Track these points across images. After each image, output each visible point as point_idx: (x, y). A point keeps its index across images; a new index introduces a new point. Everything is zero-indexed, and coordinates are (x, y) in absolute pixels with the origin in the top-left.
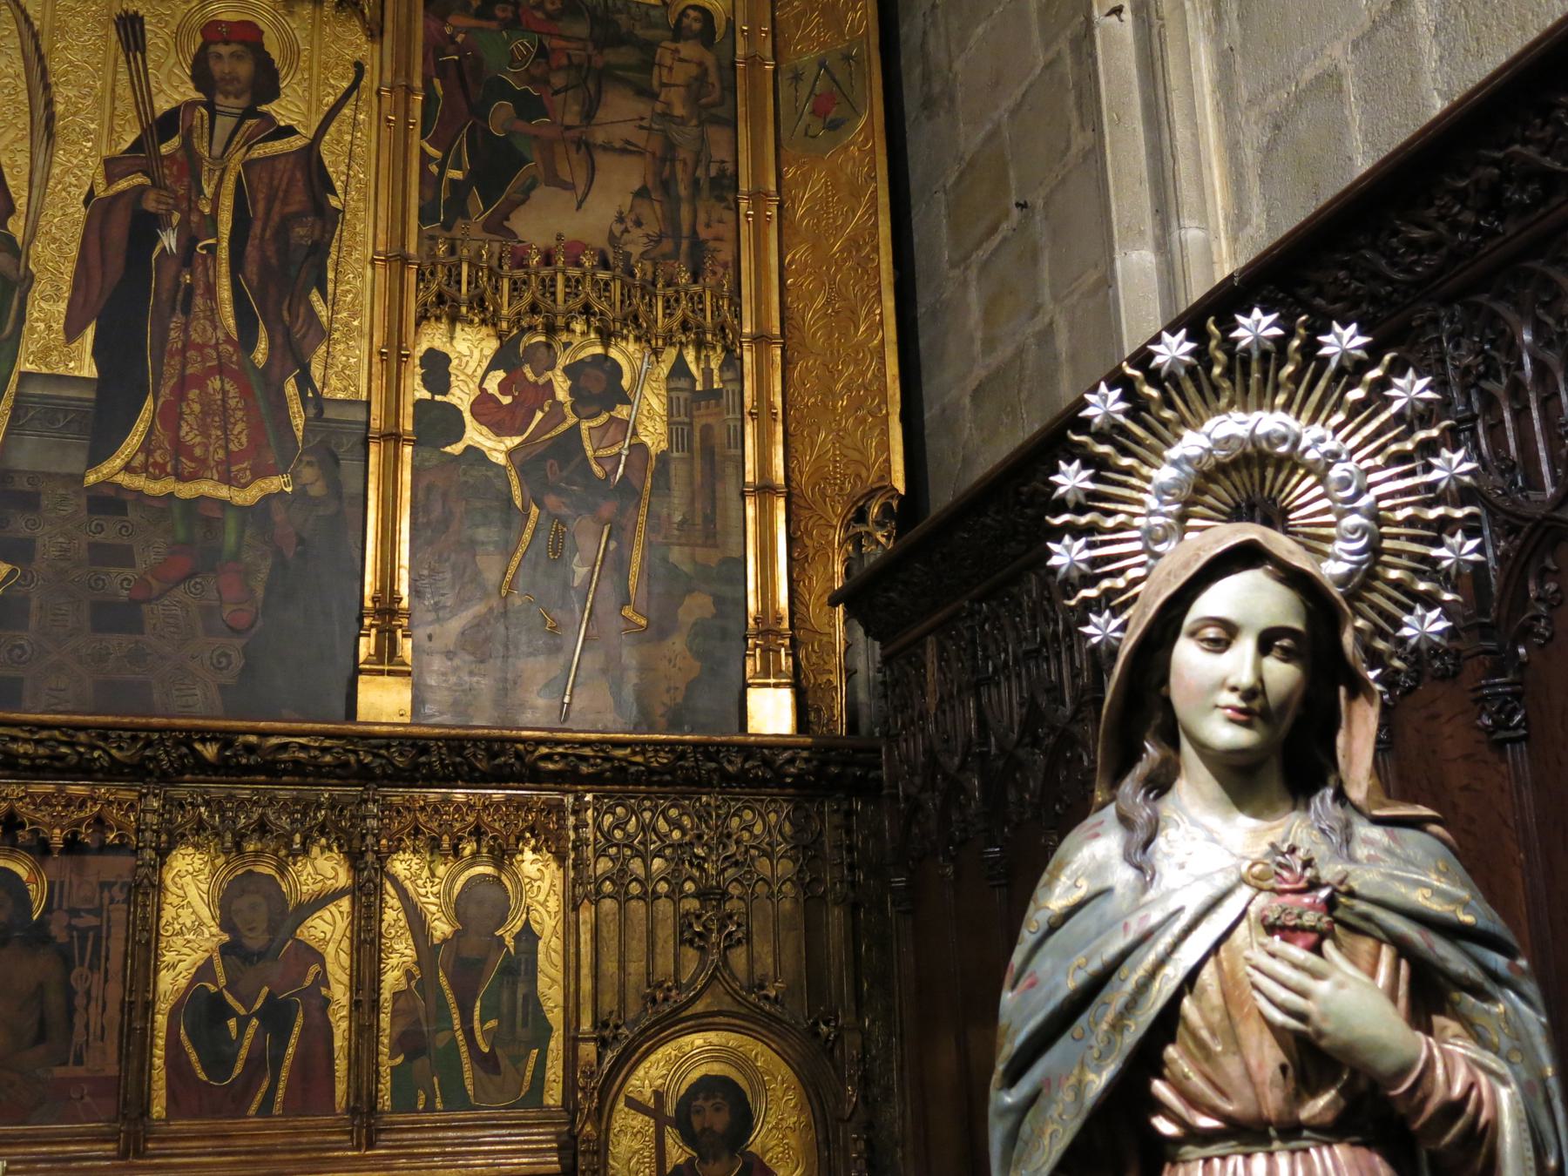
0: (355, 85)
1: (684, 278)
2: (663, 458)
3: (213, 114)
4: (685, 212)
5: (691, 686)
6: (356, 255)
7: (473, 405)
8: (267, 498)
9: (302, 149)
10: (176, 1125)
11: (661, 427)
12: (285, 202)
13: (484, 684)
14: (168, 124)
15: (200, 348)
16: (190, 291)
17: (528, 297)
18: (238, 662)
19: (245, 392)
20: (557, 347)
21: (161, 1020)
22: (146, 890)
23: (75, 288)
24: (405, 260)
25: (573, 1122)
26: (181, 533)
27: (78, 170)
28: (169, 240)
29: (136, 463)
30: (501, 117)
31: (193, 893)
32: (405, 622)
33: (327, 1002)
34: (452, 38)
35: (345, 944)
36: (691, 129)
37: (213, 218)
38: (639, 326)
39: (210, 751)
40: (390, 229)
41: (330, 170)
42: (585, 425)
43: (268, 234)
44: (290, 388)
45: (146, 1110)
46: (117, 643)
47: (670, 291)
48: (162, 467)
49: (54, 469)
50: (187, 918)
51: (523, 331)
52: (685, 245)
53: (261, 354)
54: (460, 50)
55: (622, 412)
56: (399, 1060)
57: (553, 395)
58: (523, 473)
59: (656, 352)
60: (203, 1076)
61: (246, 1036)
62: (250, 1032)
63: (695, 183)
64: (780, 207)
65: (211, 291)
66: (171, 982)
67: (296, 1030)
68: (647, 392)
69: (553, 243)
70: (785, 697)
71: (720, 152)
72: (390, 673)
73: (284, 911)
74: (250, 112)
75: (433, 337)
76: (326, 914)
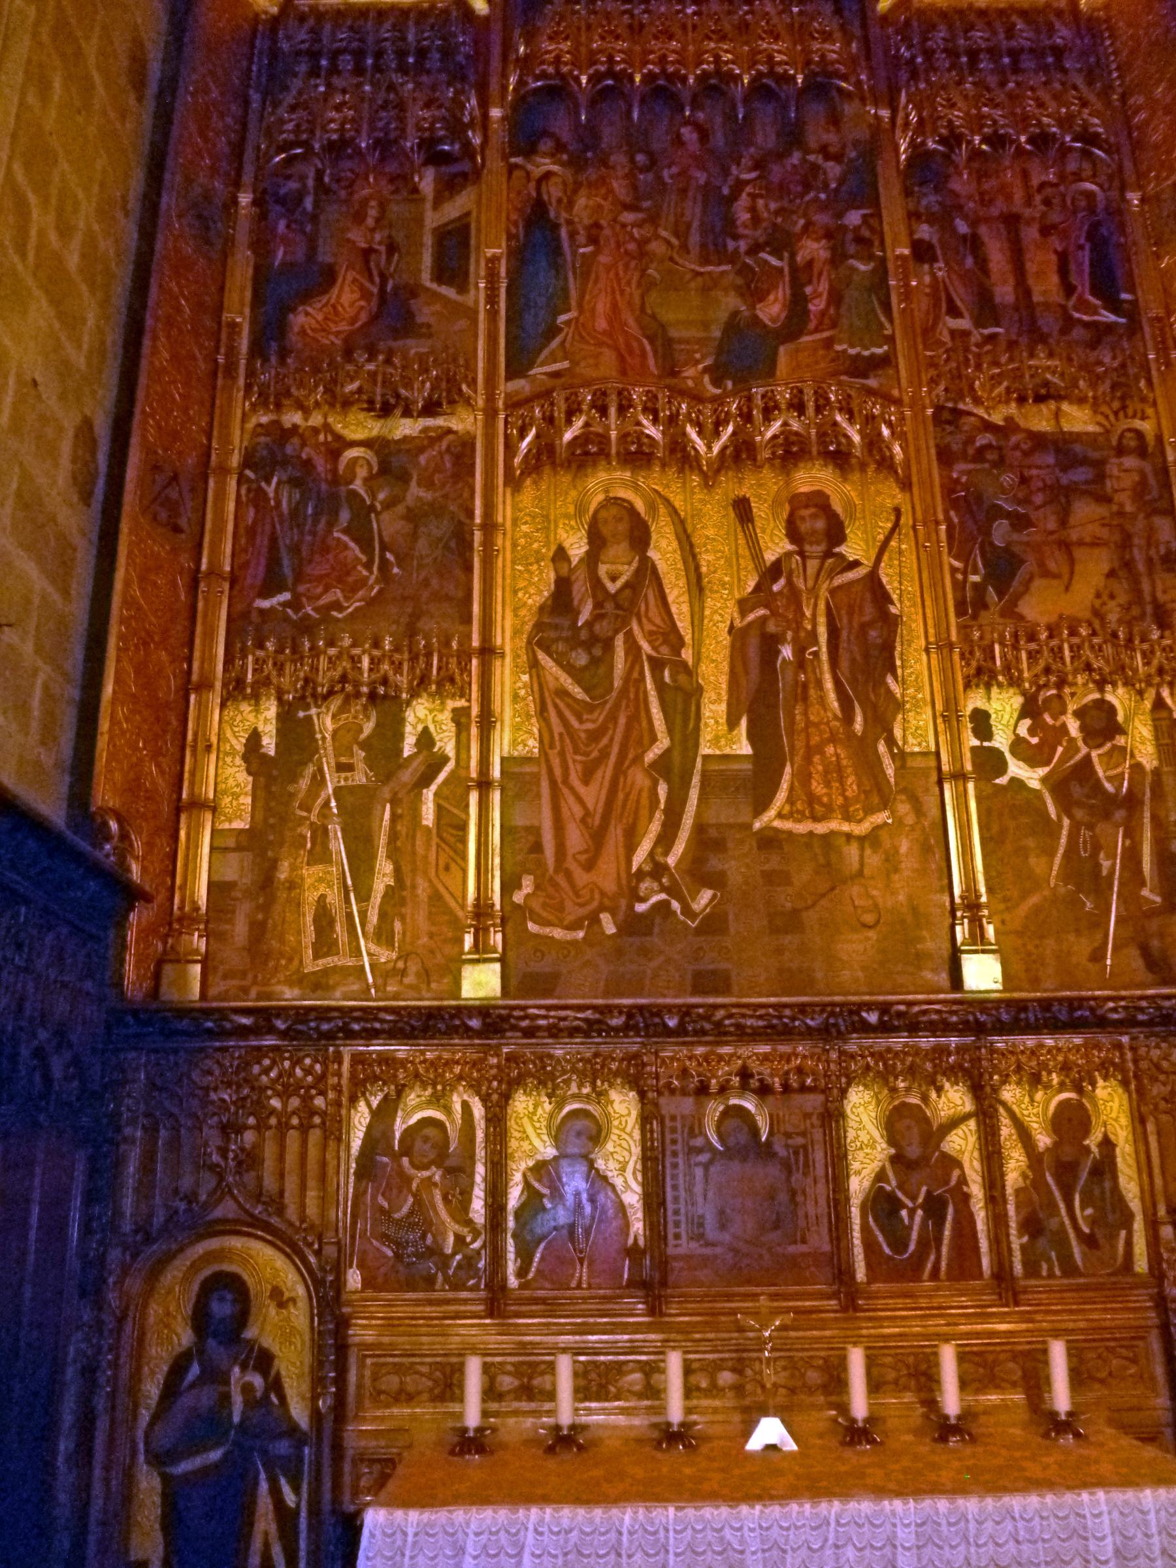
0: (896, 525)
2: (1156, 772)
4: (1146, 586)
8: (877, 828)
10: (875, 1287)
11: (1150, 749)
12: (861, 614)
14: (776, 570)
15: (816, 725)
16: (805, 686)
17: (1042, 664)
20: (1068, 699)
21: (855, 1212)
24: (951, 646)
25: (1160, 1285)
27: (722, 612)
28: (787, 652)
30: (1001, 533)
33: (967, 1197)
35: (976, 1154)
40: (937, 626)
42: (1094, 754)
44: (882, 748)
45: (853, 1277)
46: (789, 940)
47: (1145, 646)
48: (802, 813)
50: (864, 1137)
51: (1039, 688)
52: (1149, 609)
54: (966, 487)
55: (1120, 740)
56: (1025, 1239)
59: (1141, 693)
60: (887, 1250)
61: (915, 1221)
63: (1150, 561)
65: (819, 684)
66: (858, 1185)
67: (949, 1218)
68: (1137, 723)
69: (1053, 618)
74: (828, 554)
75: (975, 700)
76: (959, 1131)
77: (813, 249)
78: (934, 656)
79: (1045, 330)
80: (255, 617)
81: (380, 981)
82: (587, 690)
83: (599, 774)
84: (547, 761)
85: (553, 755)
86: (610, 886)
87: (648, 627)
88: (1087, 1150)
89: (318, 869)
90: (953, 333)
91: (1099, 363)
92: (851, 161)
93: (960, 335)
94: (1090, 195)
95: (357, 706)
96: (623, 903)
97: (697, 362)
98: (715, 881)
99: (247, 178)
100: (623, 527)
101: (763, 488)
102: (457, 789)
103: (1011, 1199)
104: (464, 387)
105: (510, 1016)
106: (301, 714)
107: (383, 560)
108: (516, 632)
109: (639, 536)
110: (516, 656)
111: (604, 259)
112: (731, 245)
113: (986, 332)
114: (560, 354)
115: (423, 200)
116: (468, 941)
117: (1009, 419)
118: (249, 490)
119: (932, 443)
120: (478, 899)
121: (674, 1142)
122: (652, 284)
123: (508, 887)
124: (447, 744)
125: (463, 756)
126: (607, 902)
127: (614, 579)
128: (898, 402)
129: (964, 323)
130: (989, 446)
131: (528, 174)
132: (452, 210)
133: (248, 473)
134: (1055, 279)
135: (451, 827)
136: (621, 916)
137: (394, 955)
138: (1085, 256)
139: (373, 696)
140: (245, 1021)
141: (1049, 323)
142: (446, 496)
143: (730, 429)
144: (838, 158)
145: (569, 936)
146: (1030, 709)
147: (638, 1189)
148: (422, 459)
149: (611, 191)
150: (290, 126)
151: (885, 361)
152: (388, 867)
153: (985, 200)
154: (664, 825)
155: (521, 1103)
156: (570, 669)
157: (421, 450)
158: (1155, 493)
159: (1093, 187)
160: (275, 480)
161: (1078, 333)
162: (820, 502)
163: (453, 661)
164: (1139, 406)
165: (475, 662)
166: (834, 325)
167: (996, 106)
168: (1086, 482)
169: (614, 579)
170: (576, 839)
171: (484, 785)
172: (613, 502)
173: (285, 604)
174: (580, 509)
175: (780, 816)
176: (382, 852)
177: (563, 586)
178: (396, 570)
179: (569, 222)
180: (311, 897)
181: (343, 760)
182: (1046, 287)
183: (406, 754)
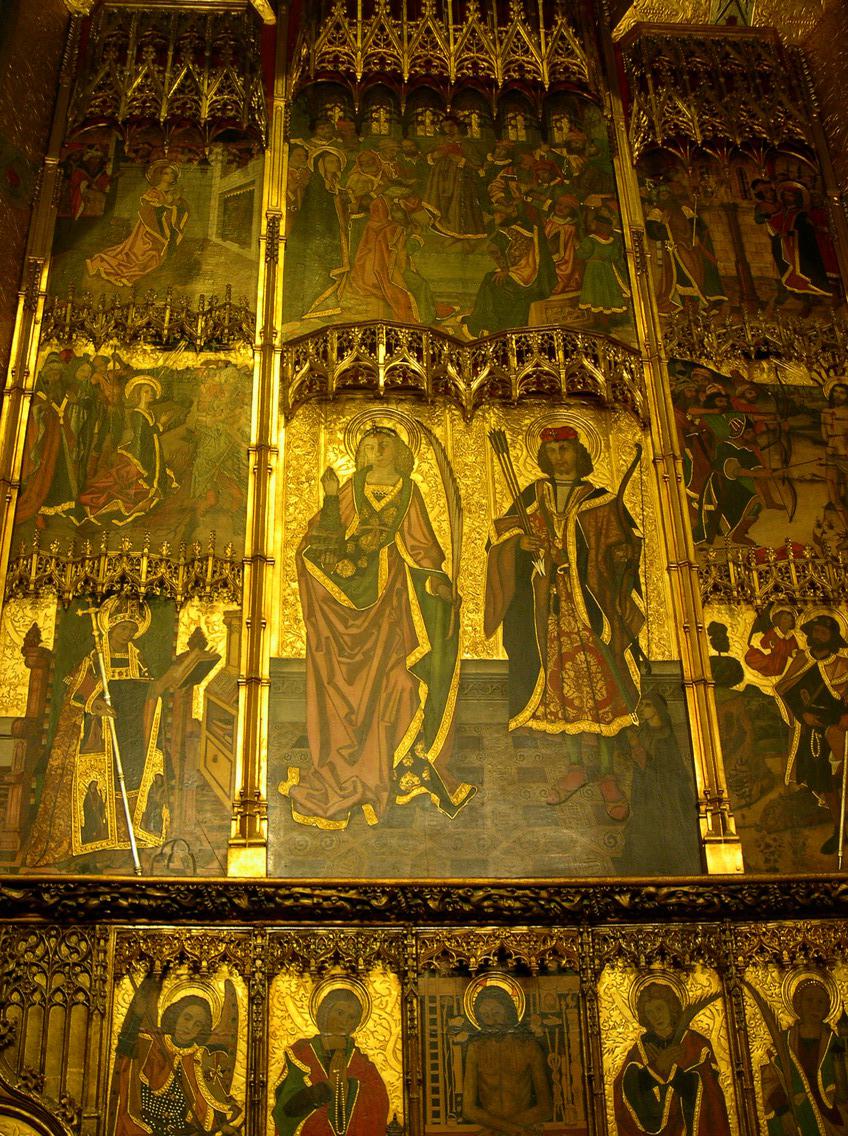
0: (638, 458)
3: (555, 485)
7: (746, 657)
8: (623, 731)
9: (612, 501)
12: (607, 537)
14: (528, 495)
15: (569, 635)
16: (557, 598)
17: (771, 584)
19: (601, 662)
21: (609, 1089)
22: (588, 998)
23: (487, 603)
24: (690, 566)
27: (479, 530)
28: (540, 567)
29: (538, 713)
30: (730, 469)
31: (619, 1002)
33: (716, 1074)
34: (692, 421)
35: (723, 1032)
37: (565, 550)
39: (624, 900)
41: (631, 513)
42: (821, 665)
43: (600, 558)
48: (555, 714)
49: (489, 721)
50: (616, 1017)
53: (606, 635)
54: (699, 428)
56: (772, 1115)
57: (797, 646)
58: (786, 698)
60: (641, 1128)
62: (669, 1097)
65: (570, 597)
69: (781, 544)
72: (726, 842)
73: (679, 1012)
75: (715, 614)
77: (560, 224)
79: (763, 298)
82: (351, 597)
83: (364, 673)
84: (314, 660)
85: (320, 657)
86: (372, 781)
87: (411, 542)
88: (828, 1028)
89: (90, 758)
90: (682, 298)
92: (591, 155)
96: (385, 795)
97: (459, 313)
102: (227, 687)
103: (757, 1076)
105: (276, 894)
106: (80, 613)
107: (163, 472)
108: (286, 544)
110: (285, 565)
111: (375, 224)
112: (487, 218)
116: (235, 827)
117: (735, 373)
120: (245, 788)
121: (433, 1022)
122: (416, 247)
123: (277, 776)
124: (218, 640)
125: (234, 654)
126: (370, 795)
127: (379, 498)
128: (637, 353)
129: (694, 291)
130: (718, 394)
133: (40, 394)
134: (769, 258)
135: (220, 718)
140: (15, 894)
141: (763, 294)
143: (486, 372)
144: (580, 152)
146: (762, 624)
147: (399, 1068)
154: (424, 723)
155: (286, 985)
156: (336, 578)
159: (799, 186)
160: (65, 401)
161: (790, 303)
162: (567, 435)
165: (247, 569)
166: (579, 287)
167: (715, 115)
168: (803, 428)
169: (379, 498)
170: (340, 735)
171: (253, 681)
173: (68, 512)
175: (534, 716)
176: (153, 742)
177: (331, 501)
178: (175, 485)
181: (118, 656)
182: (762, 264)
183: (179, 652)
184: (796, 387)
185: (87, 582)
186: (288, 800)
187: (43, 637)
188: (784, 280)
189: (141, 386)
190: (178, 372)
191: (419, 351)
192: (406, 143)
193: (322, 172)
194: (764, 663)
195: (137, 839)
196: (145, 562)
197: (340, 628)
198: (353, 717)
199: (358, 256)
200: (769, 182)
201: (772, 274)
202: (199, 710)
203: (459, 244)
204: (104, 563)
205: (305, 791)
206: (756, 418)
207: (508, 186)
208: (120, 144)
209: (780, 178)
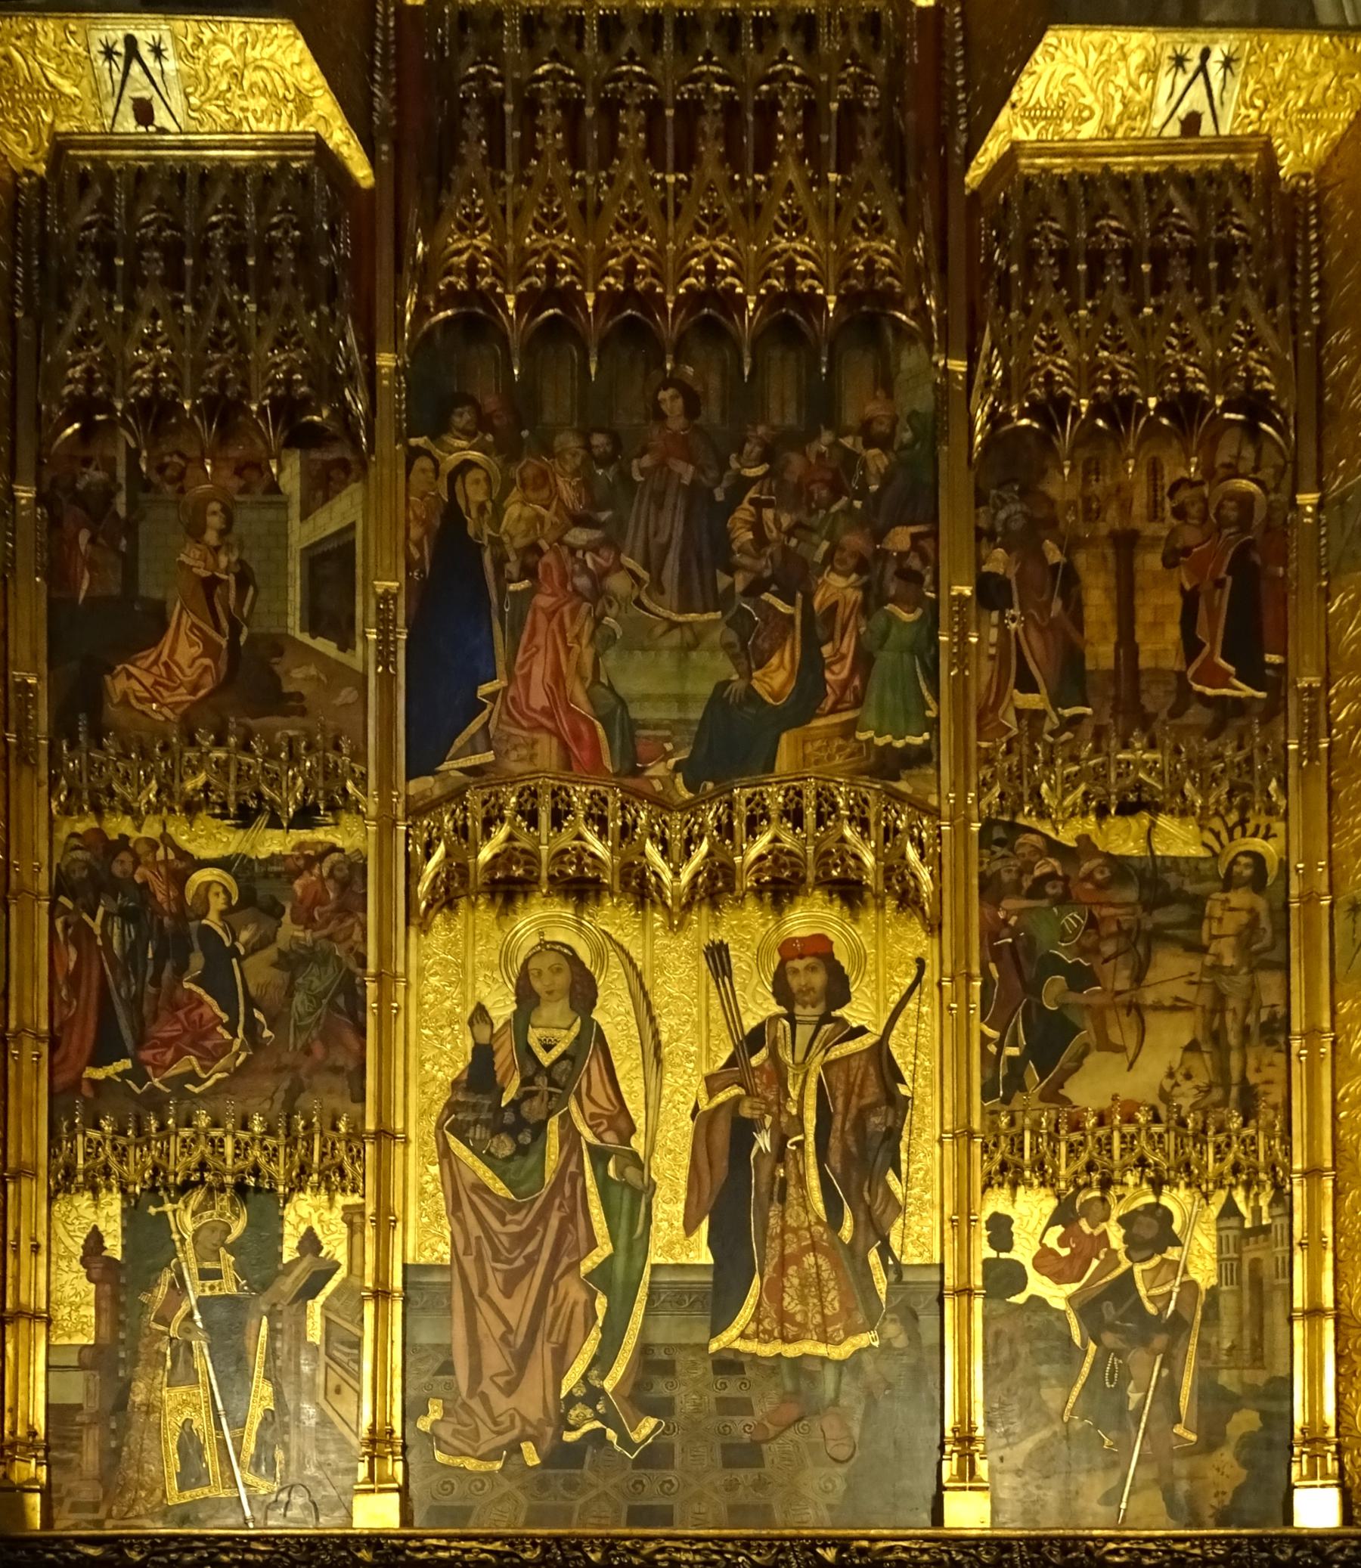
1: (1235, 1124)
2: (1213, 1293)
4: (1235, 1061)
5: (1239, 1492)
6: (925, 1136)
12: (861, 1096)
13: (1052, 1496)
14: (755, 1039)
15: (795, 1231)
16: (784, 1182)
17: (1084, 1157)
18: (841, 1486)
19: (835, 1265)
23: (690, 1189)
24: (971, 1135)
26: (789, 1385)
27: (684, 1090)
28: (764, 1141)
30: (1054, 991)
32: (981, 1447)
34: (1005, 921)
36: (1242, 978)
37: (800, 1117)
38: (1189, 1173)
40: (955, 1110)
42: (1138, 1269)
44: (874, 1258)
46: (745, 1475)
48: (770, 1333)
51: (1079, 1189)
52: (1234, 1092)
53: (846, 1232)
54: (1014, 932)
55: (1173, 1253)
57: (1107, 1244)
59: (1206, 1196)
63: (1245, 1031)
64: (1334, 1043)
65: (802, 1181)
68: (1197, 1233)
69: (1107, 1103)
70: (1333, 1495)
71: (1271, 996)
74: (826, 1018)
75: (997, 1202)
77: (837, 587)
78: (948, 1147)
79: (1150, 708)
80: (87, 1091)
81: (259, 1516)
82: (510, 1186)
83: (525, 1282)
85: (468, 1262)
86: (534, 1413)
90: (1020, 713)
91: (1218, 757)
92: (904, 447)
93: (1037, 716)
94: (1245, 501)
95: (223, 1201)
96: (550, 1431)
97: (668, 755)
98: (661, 1409)
99: (26, 461)
100: (563, 980)
101: (748, 930)
104: (349, 784)
106: (152, 1210)
107: (249, 1016)
108: (423, 1114)
109: (583, 992)
111: (543, 601)
113: (1067, 712)
114: (480, 741)
115: (285, 506)
116: (363, 1470)
117: (1084, 839)
118: (66, 926)
119: (975, 870)
120: (374, 1424)
124: (335, 1245)
125: (357, 1261)
127: (548, 1048)
128: (935, 813)
129: (1033, 701)
130: (1052, 876)
131: (436, 463)
132: (329, 520)
133: (62, 899)
134: (1173, 632)
136: (546, 1446)
137: (276, 1487)
138: (1223, 600)
139: (241, 1189)
141: (1156, 699)
142: (330, 937)
143: (705, 847)
144: (885, 443)
145: (485, 1466)
148: (298, 885)
149: (555, 493)
150: (77, 372)
151: (925, 756)
152: (267, 1390)
153: (1091, 512)
156: (489, 1159)
157: (298, 873)
158: (1266, 941)
159: (1253, 487)
161: (1196, 715)
162: (819, 949)
163: (341, 1146)
164: (1263, 820)
165: (369, 1148)
166: (858, 703)
169: (548, 1048)
170: (495, 1360)
172: (546, 946)
174: (506, 957)
175: (743, 1335)
176: (258, 1371)
177: (483, 1055)
178: (267, 1033)
179: (496, 542)
180: (173, 1423)
181: (208, 1265)
182: (1160, 645)
184: (1175, 859)
185: (156, 1170)
186: (432, 1437)
187: (107, 1243)
188: (1190, 673)
189: (208, 885)
190: (261, 862)
191: (602, 821)
192: (598, 440)
193: (461, 502)
194: (1061, 1266)
195: (246, 1485)
196: (229, 1143)
197: (495, 1225)
198: (511, 1338)
199: (520, 659)
200: (1201, 483)
201: (1173, 662)
202: (315, 1331)
203: (676, 633)
204: (174, 1147)
205: (450, 1428)
206: (1107, 911)
207: (759, 516)
208: (133, 455)
209: (1221, 472)
